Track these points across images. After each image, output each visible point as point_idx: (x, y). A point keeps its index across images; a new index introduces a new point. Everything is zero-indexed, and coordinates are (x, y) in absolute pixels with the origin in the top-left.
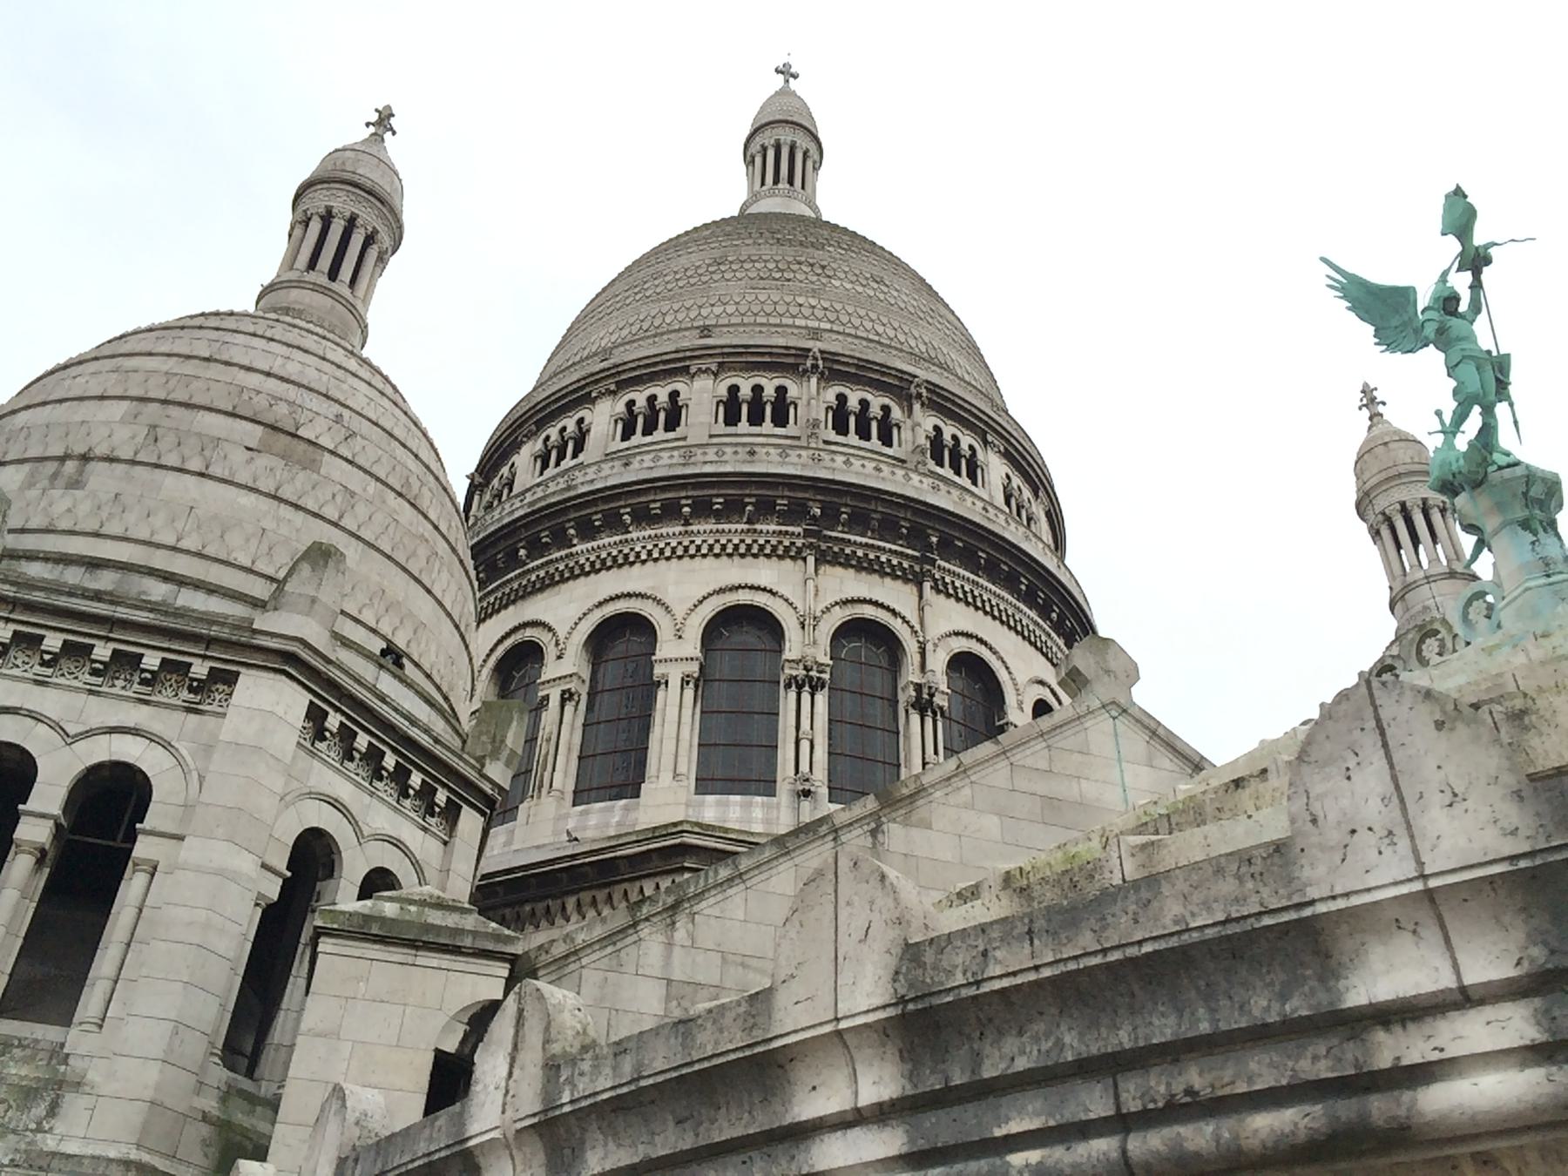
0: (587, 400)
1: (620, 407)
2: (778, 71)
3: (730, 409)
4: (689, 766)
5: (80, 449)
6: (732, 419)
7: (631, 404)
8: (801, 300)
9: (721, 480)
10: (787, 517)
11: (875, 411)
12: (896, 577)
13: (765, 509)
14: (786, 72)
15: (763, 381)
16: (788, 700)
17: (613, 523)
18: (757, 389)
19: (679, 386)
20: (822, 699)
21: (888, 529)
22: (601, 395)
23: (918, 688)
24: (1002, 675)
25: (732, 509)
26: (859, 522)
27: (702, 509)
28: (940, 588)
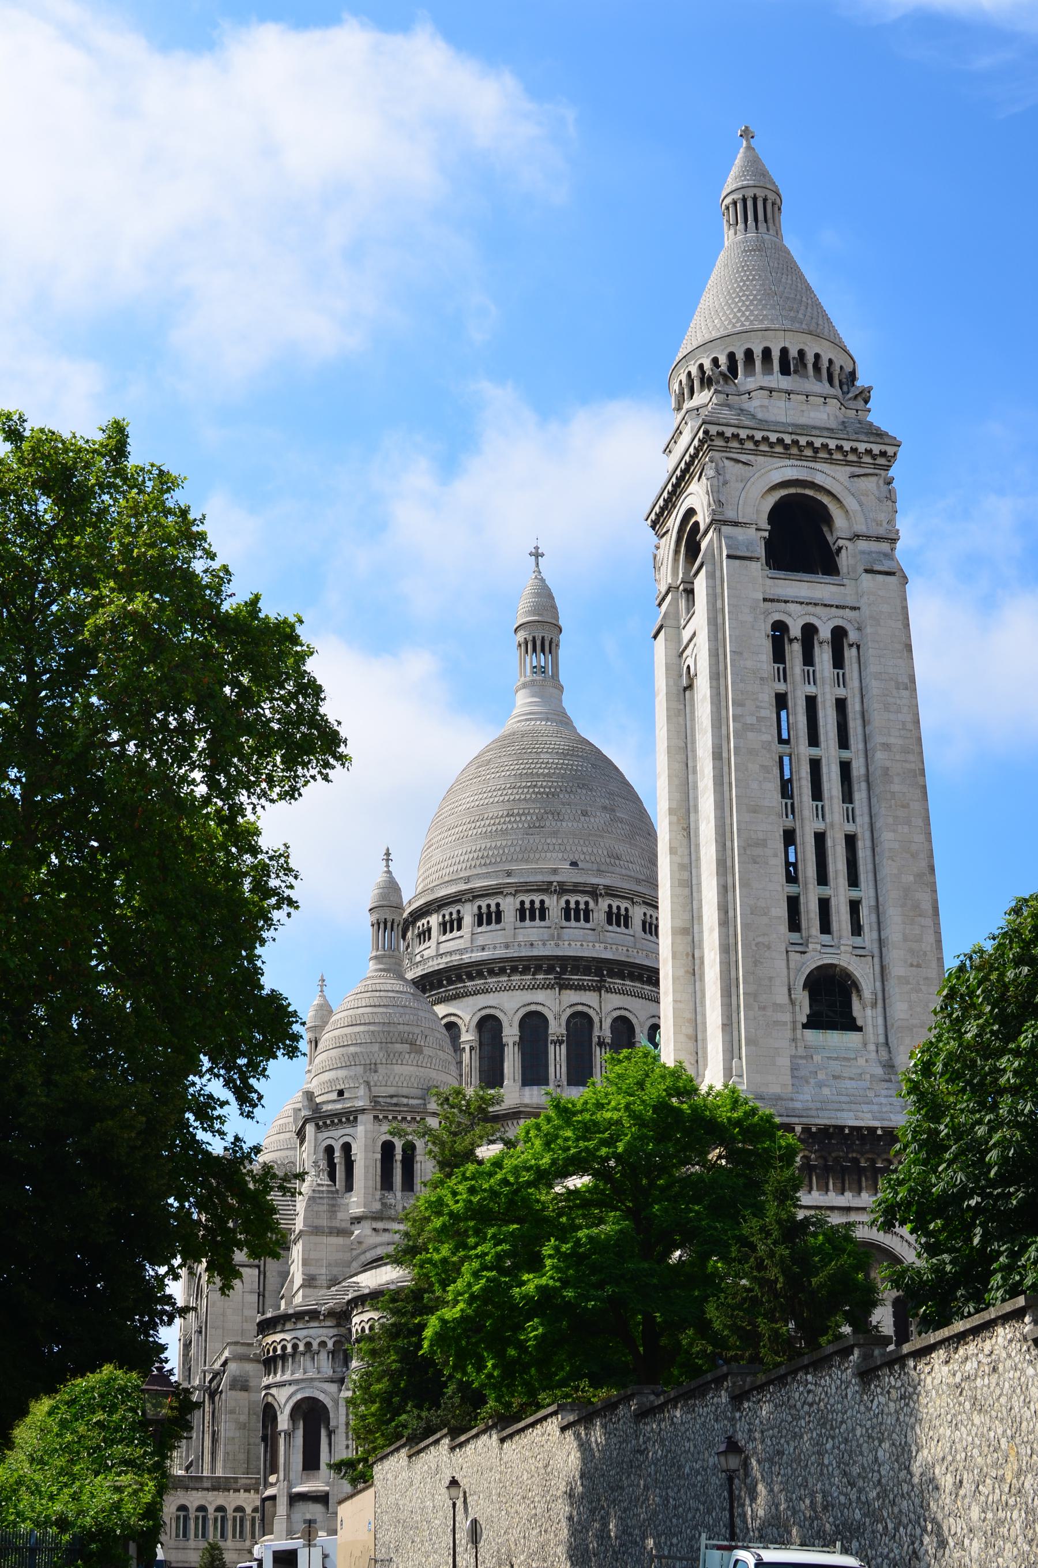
0: (459, 901)
1: (476, 910)
2: (531, 554)
3: (522, 913)
4: (519, 1077)
5: (373, 1061)
6: (523, 919)
7: (480, 907)
8: (548, 841)
9: (521, 959)
10: (547, 973)
11: (582, 906)
12: (590, 990)
13: (538, 969)
14: (537, 555)
15: (534, 898)
16: (551, 1048)
17: (480, 975)
18: (532, 902)
19: (499, 900)
20: (564, 1047)
21: (587, 971)
22: (466, 901)
23: (599, 1037)
24: (634, 1021)
25: (526, 971)
26: (575, 970)
27: (514, 970)
28: (609, 991)
